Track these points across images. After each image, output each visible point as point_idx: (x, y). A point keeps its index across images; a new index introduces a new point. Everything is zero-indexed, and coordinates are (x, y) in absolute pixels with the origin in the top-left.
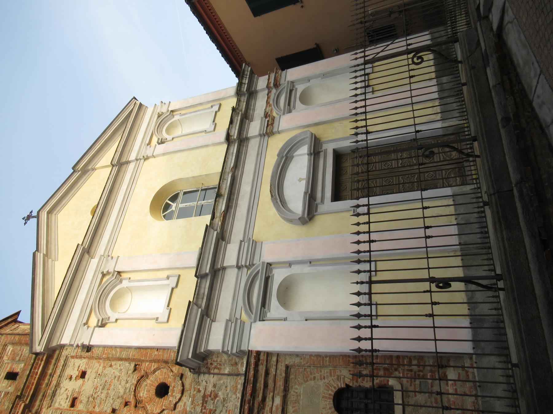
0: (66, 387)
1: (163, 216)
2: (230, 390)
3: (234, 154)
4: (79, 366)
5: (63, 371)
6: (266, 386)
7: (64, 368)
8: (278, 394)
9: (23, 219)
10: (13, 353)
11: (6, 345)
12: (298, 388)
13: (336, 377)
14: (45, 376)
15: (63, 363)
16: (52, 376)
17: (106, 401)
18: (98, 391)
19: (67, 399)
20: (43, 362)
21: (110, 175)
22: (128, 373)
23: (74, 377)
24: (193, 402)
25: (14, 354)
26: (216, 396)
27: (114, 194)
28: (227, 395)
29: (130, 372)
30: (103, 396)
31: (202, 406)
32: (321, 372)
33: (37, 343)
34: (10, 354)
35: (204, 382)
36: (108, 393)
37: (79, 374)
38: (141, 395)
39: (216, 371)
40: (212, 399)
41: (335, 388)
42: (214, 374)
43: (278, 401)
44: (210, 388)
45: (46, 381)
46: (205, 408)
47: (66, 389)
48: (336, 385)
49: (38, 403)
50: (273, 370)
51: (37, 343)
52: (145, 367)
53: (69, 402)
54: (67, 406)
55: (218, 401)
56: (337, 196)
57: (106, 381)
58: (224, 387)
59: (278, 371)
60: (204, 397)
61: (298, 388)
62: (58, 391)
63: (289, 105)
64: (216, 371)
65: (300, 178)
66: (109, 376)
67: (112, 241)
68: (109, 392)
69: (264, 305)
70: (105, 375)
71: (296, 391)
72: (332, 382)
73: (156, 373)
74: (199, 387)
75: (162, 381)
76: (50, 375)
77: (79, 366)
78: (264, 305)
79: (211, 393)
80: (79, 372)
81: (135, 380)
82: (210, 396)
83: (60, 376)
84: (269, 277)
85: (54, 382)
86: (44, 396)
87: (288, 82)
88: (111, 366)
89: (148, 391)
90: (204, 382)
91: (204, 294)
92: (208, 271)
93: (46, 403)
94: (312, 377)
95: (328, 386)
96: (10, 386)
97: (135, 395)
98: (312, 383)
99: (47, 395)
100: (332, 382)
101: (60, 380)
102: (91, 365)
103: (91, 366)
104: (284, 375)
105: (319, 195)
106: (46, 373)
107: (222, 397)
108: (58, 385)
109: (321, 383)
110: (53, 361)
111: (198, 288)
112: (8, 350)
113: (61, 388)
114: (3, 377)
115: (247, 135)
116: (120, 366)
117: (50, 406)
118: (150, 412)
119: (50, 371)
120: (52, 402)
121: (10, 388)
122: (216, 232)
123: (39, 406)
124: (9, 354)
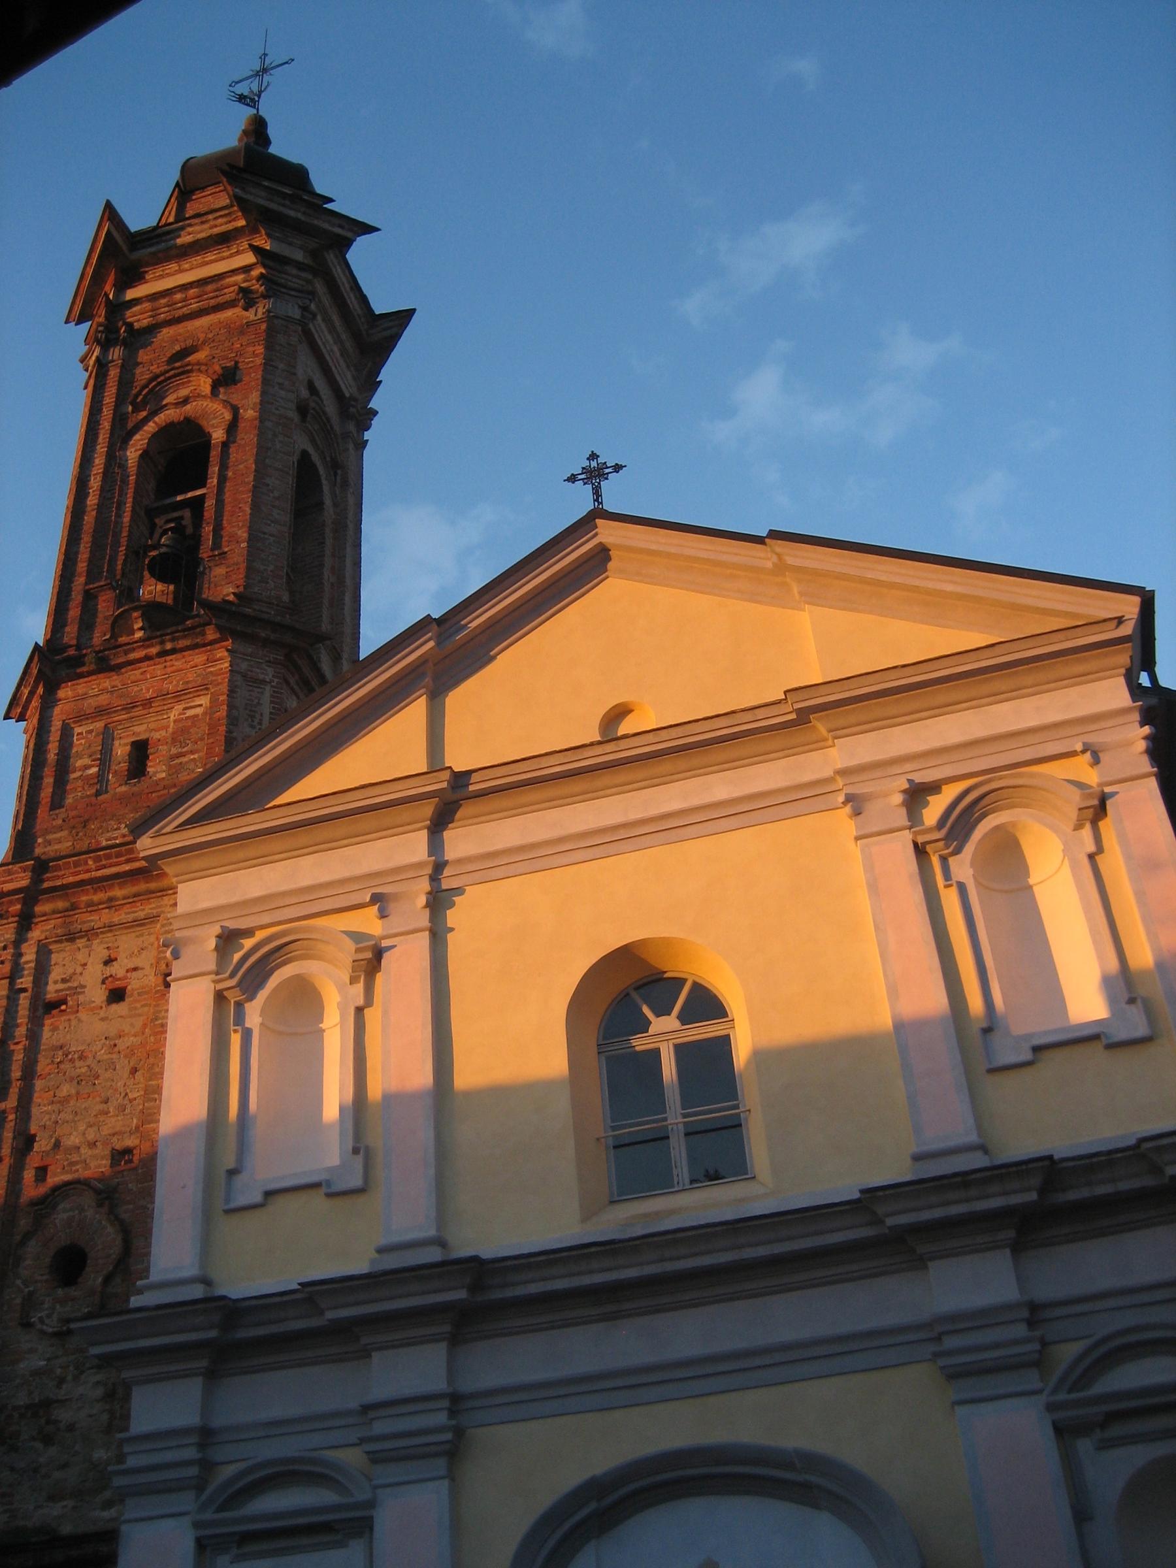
0: (89, 966)
4: (135, 969)
7: (133, 926)
9: (593, 456)
11: (207, 689)
14: (101, 889)
15: (141, 914)
16: (111, 904)
18: (78, 1064)
19: (64, 981)
20: (127, 867)
21: (743, 710)
23: (109, 971)
24: (37, 1373)
26: (48, 1440)
27: (682, 763)
30: (66, 1089)
34: (187, 718)
36: (67, 1099)
37: (119, 979)
53: (57, 991)
60: (47, 1404)
62: (81, 943)
68: (72, 1103)
69: (247, 1538)
73: (110, 1229)
74: (70, 1378)
76: (111, 899)
77: (135, 969)
80: (125, 978)
81: (96, 1167)
82: (48, 1422)
83: (110, 927)
88: (134, 1071)
92: (330, 1315)
101: (102, 933)
102: (138, 1005)
103: (136, 1008)
106: (111, 887)
107: (42, 1460)
110: (143, 886)
115: (932, 1259)
119: (118, 892)
122: (461, 1294)
124: (190, 713)
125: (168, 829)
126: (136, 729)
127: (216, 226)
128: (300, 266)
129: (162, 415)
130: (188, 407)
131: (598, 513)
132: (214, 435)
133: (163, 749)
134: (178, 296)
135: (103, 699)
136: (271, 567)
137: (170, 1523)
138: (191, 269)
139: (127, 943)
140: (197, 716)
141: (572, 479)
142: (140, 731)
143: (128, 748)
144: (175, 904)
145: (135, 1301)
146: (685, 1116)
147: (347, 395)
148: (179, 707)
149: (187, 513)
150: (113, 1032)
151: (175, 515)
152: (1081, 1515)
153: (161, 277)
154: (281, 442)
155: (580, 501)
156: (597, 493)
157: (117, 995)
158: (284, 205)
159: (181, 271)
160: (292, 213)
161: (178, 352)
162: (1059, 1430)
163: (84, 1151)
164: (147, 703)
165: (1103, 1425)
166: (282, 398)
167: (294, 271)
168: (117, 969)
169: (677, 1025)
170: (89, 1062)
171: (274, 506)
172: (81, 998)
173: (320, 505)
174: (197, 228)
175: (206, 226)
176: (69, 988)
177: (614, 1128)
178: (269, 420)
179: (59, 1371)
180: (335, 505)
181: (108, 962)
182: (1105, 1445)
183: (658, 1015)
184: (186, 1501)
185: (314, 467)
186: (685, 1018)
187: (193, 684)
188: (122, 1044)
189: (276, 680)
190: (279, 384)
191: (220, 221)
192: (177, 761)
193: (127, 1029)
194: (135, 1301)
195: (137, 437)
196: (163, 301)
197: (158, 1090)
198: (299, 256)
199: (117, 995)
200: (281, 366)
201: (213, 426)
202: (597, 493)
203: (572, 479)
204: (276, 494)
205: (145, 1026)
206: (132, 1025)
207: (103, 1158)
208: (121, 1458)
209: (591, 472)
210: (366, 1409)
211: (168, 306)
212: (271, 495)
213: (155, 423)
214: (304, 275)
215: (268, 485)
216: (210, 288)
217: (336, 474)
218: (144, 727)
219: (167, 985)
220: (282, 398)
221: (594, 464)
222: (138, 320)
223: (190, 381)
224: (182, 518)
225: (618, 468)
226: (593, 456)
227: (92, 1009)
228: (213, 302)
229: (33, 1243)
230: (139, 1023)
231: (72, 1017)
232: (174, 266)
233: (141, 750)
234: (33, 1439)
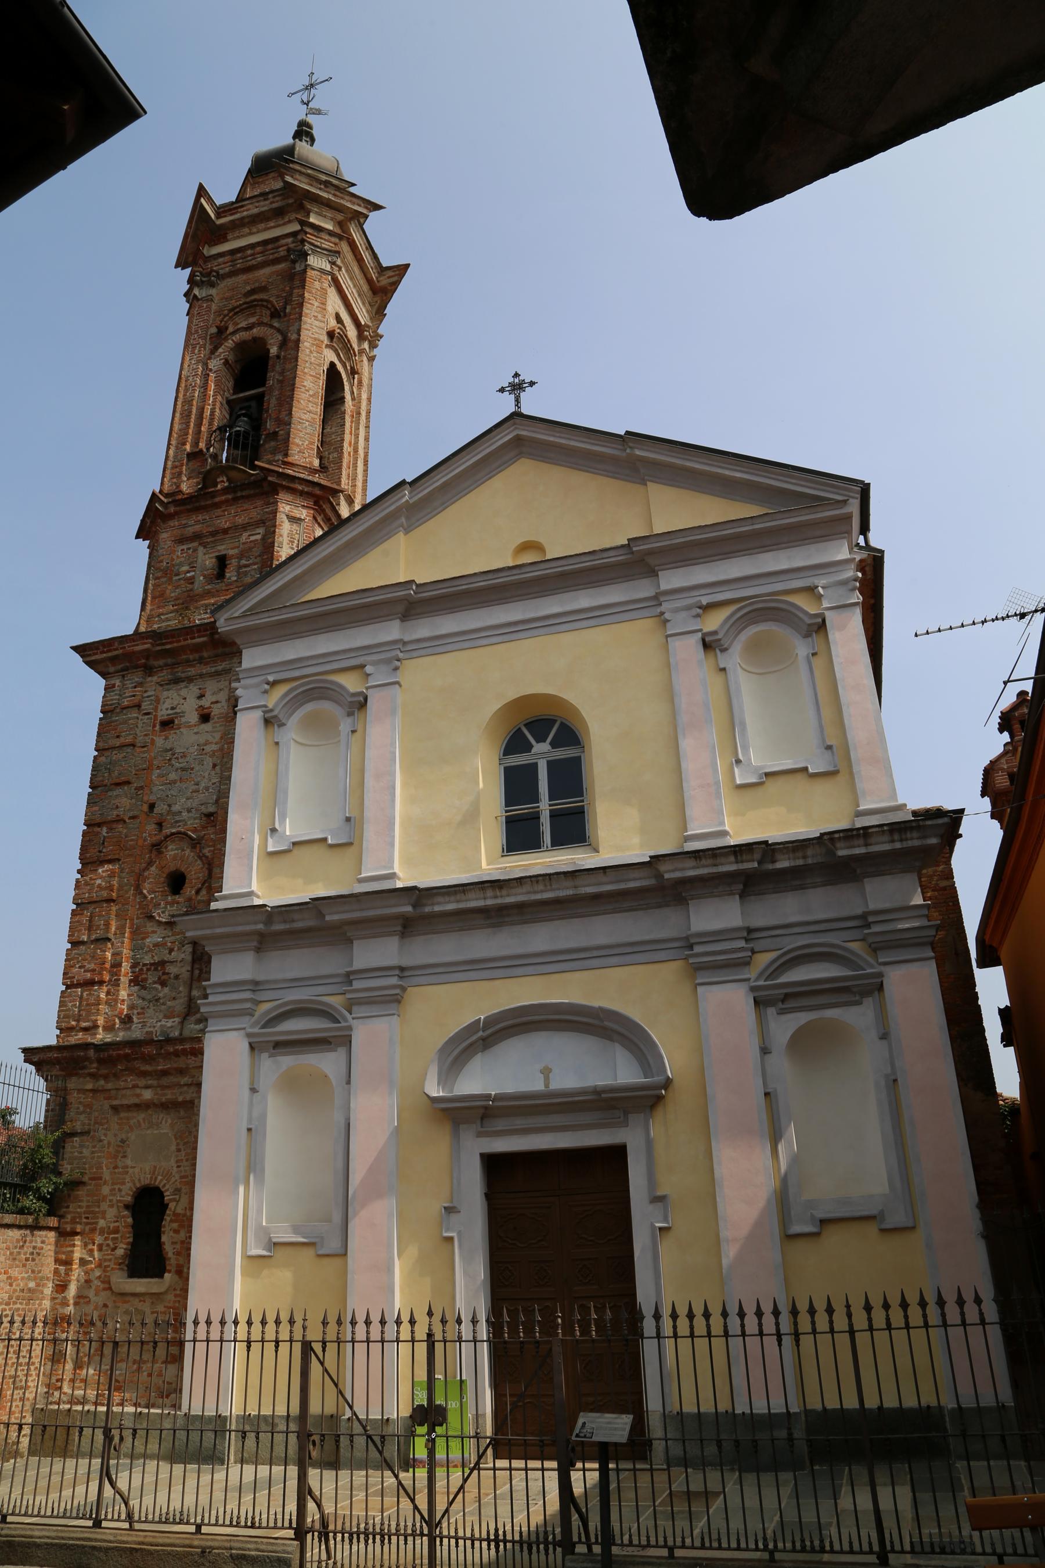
0: (187, 700)
1: (520, 728)
2: (170, 1007)
3: (622, 886)
4: (217, 702)
5: (211, 676)
6: (165, 1073)
8: (156, 1094)
9: (516, 375)
10: (252, 545)
12: (168, 1124)
13: (179, 1187)
15: (220, 668)
17: (166, 784)
18: (180, 761)
19: (173, 708)
22: (202, 805)
24: (156, 945)
25: (250, 549)
26: (163, 984)
28: (164, 1004)
29: (203, 809)
30: (173, 776)
31: (151, 964)
32: (187, 1160)
33: (226, 616)
34: (251, 542)
35: (183, 956)
36: (174, 782)
38: (170, 848)
39: (197, 972)
40: (159, 978)
41: (164, 1186)
42: (192, 971)
43: (147, 1095)
44: (173, 970)
45: (191, 657)
46: (148, 970)
47: (185, 699)
48: (167, 1187)
49: (161, 662)
50: (186, 1079)
51: (226, 616)
52: (209, 834)
53: (168, 715)
54: (162, 716)
55: (157, 989)
56: (493, 1164)
57: (192, 769)
58: (174, 994)
59: (185, 1088)
60: (163, 963)
61: (168, 1124)
62: (183, 685)
63: (786, 997)
64: (197, 972)
65: (550, 1070)
66: (199, 771)
67: (437, 644)
68: (178, 783)
69: (277, 1045)
70: (201, 763)
71: (163, 1122)
72: (173, 1180)
74: (176, 949)
75: (188, 876)
77: (217, 702)
78: (277, 1045)
79: (168, 974)
80: (210, 707)
82: (164, 974)
83: (201, 676)
84: (330, 1043)
85: (192, 671)
86: (172, 666)
87: (880, 975)
88: (214, 766)
89: (174, 858)
90: (183, 956)
91: (293, 921)
92: (328, 918)
93: (165, 675)
94: (181, 1147)
95: (168, 1175)
96: (205, 576)
97: (167, 837)
98: (173, 1148)
99: (176, 670)
100: (173, 1180)
102: (218, 725)
104: (180, 1099)
105: (501, 1124)
107: (161, 995)
108: (190, 680)
109: (173, 1162)
111: (298, 907)
112: (258, 531)
113: (186, 687)
114: (219, 551)
116: (213, 784)
117: (161, 685)
118: (146, 874)
120: (167, 684)
121: (202, 578)
123: (160, 667)
124: (252, 538)
125: (236, 615)
126: (219, 548)
127: (273, 202)
128: (331, 233)
129: (237, 336)
130: (255, 330)
131: (517, 416)
132: (272, 351)
133: (234, 562)
134: (249, 252)
135: (197, 528)
136: (307, 442)
137: (235, 1033)
138: (258, 232)
139: (211, 685)
140: (257, 540)
141: (502, 390)
142: (222, 549)
143: (214, 560)
144: (240, 662)
145: (214, 906)
146: (550, 805)
147: (363, 323)
148: (245, 535)
149: (253, 404)
150: (202, 741)
151: (247, 404)
152: (765, 1051)
153: (238, 237)
155: (506, 406)
156: (517, 400)
157: (205, 718)
158: (320, 189)
159: (251, 234)
160: (325, 195)
161: (248, 291)
162: (757, 1002)
163: (185, 814)
164: (225, 531)
165: (783, 1001)
167: (327, 237)
168: (205, 702)
169: (549, 747)
170: (187, 759)
172: (183, 720)
174: (262, 203)
175: (267, 202)
176: (176, 713)
177: (506, 812)
179: (169, 944)
180: (353, 399)
181: (201, 696)
182: (781, 1012)
183: (538, 742)
184: (245, 1022)
185: (339, 373)
186: (554, 745)
187: (255, 519)
188: (208, 749)
191: (277, 199)
192: (244, 569)
193: (210, 739)
194: (214, 906)
195: (220, 350)
196: (239, 255)
197: (229, 778)
198: (329, 226)
199: (205, 718)
200: (316, 304)
201: (270, 344)
202: (517, 400)
203: (502, 390)
204: (311, 393)
205: (222, 738)
206: (214, 737)
207: (195, 819)
208: (206, 997)
209: (514, 386)
210: (348, 974)
211: (242, 258)
213: (233, 340)
214: (333, 239)
215: (305, 386)
216: (270, 246)
217: (354, 378)
218: (223, 547)
219: (235, 713)
221: (517, 380)
222: (222, 269)
223: (255, 313)
224: (250, 407)
225: (532, 384)
226: (516, 375)
227: (190, 726)
228: (271, 257)
229: (153, 869)
230: (218, 736)
231: (177, 731)
232: (246, 230)
233: (222, 561)
234: (155, 983)
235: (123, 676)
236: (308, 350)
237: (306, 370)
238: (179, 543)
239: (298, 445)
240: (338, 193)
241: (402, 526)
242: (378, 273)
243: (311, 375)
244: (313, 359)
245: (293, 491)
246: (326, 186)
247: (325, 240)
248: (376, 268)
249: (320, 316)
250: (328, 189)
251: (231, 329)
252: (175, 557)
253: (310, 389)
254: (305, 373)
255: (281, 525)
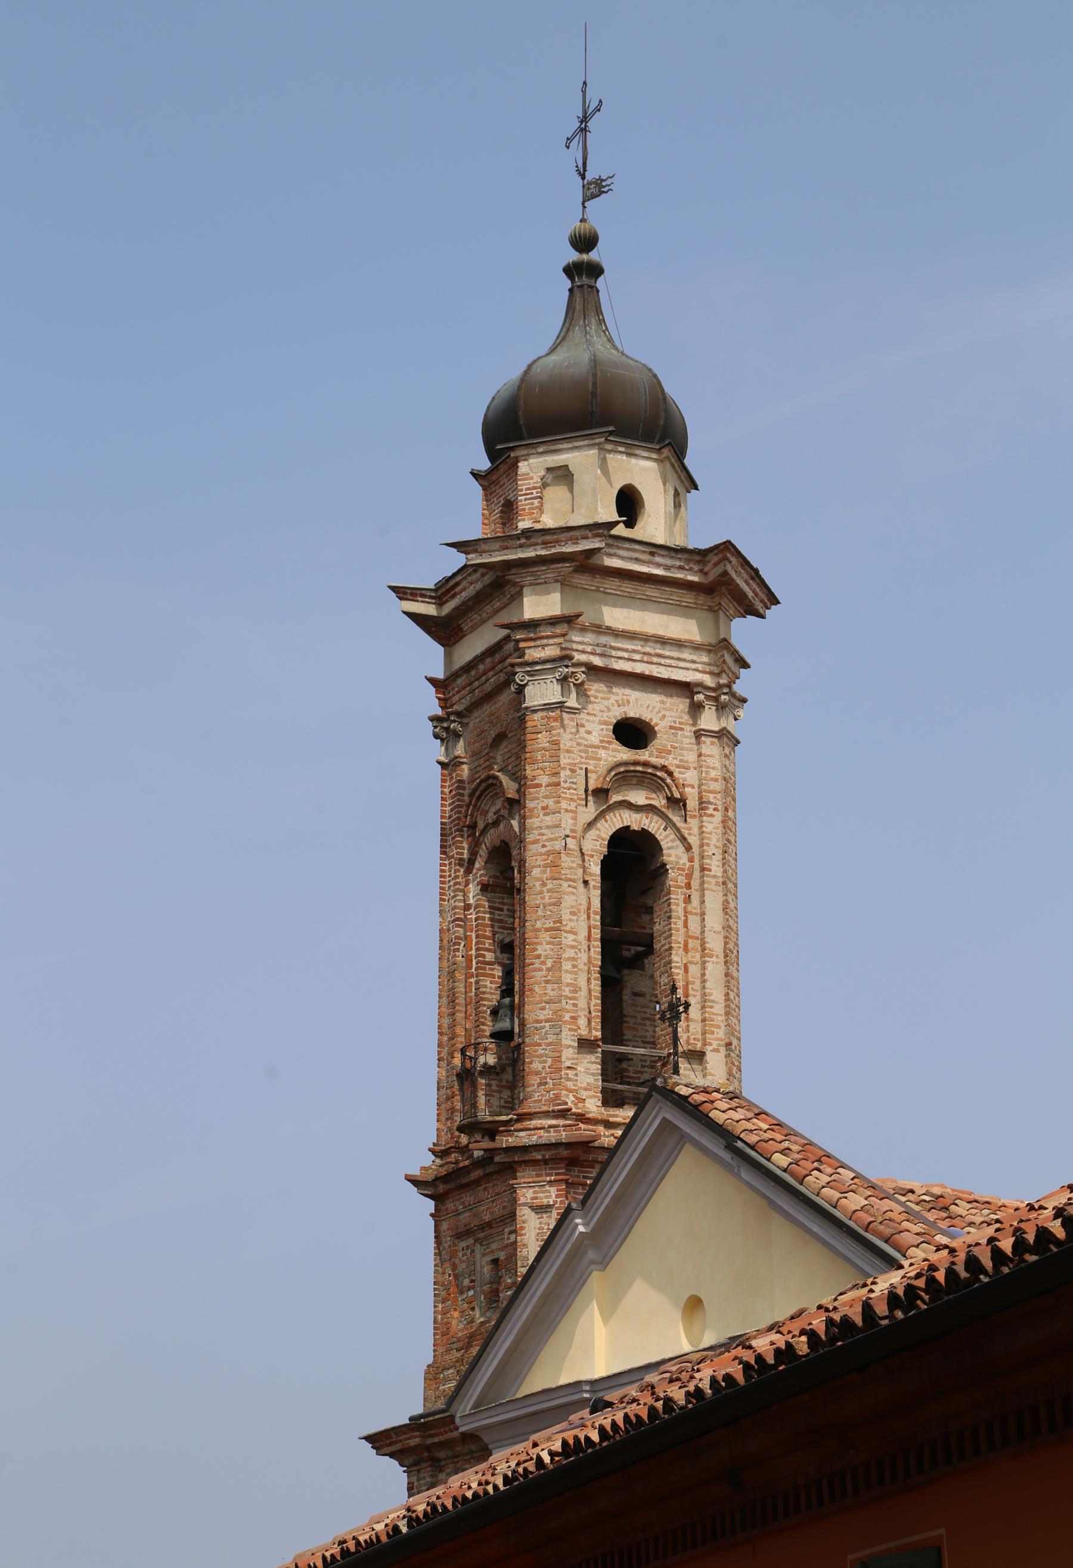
154: (549, 891)
161: (494, 740)
166: (548, 827)
171: (547, 982)
173: (663, 869)
178: (536, 867)
189: (559, 1200)
190: (543, 808)
212: (544, 967)
214: (558, 630)
215: (538, 957)
220: (548, 827)
235: (418, 1471)
236: (538, 884)
237: (539, 925)
238: (459, 1238)
239: (537, 1073)
240: (548, 538)
241: (593, 1262)
242: (698, 562)
243: (547, 930)
244: (547, 895)
245: (534, 1163)
246: (527, 538)
247: (548, 637)
248: (688, 561)
249: (550, 802)
250: (533, 540)
251: (481, 825)
252: (457, 1261)
253: (547, 957)
254: (539, 930)
255: (522, 1228)
